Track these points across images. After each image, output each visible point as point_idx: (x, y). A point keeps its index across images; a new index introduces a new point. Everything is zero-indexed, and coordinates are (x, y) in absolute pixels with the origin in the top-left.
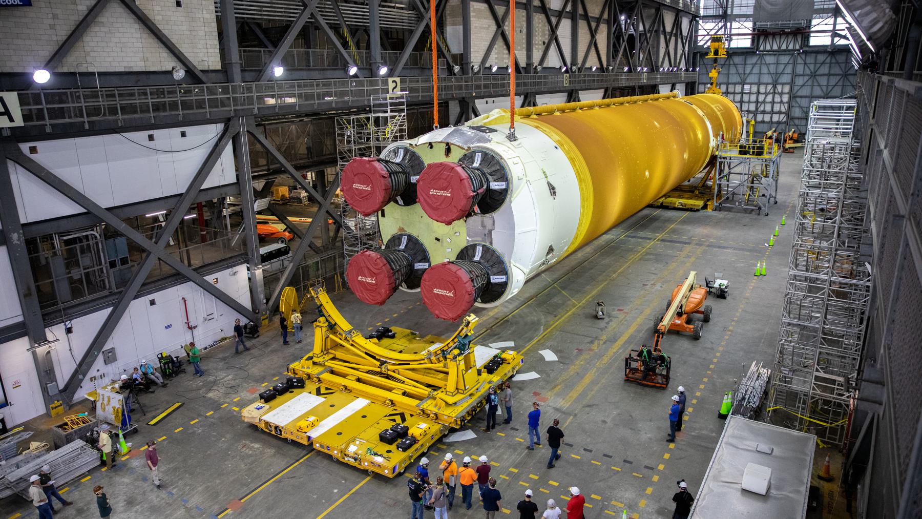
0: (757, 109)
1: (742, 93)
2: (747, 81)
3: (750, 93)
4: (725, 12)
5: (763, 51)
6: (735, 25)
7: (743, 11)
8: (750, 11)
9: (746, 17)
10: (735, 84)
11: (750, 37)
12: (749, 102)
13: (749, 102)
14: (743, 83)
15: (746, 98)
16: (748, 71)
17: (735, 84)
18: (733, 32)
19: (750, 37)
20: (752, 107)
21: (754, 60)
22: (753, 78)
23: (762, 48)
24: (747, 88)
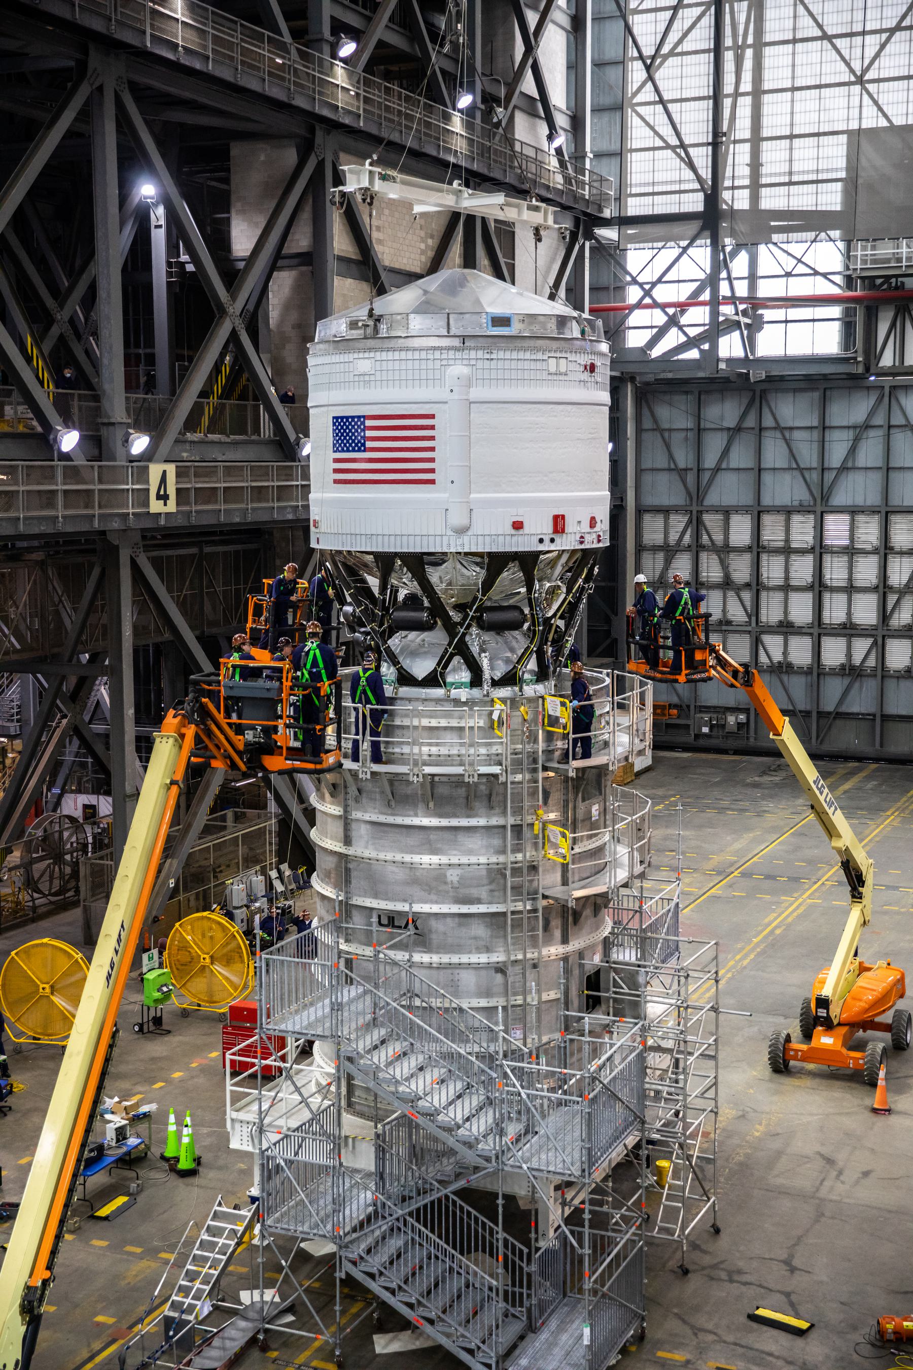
0: (884, 616)
1: (820, 550)
2: (840, 498)
3: (851, 551)
4: (712, 198)
5: (892, 372)
6: (768, 259)
7: (802, 199)
8: (831, 199)
9: (812, 222)
10: (788, 512)
11: (836, 311)
12: (850, 589)
13: (850, 589)
14: (820, 505)
15: (835, 571)
16: (837, 454)
17: (788, 512)
18: (765, 289)
19: (836, 311)
20: (866, 611)
21: (853, 410)
22: (857, 489)
23: (887, 360)
24: (837, 529)
